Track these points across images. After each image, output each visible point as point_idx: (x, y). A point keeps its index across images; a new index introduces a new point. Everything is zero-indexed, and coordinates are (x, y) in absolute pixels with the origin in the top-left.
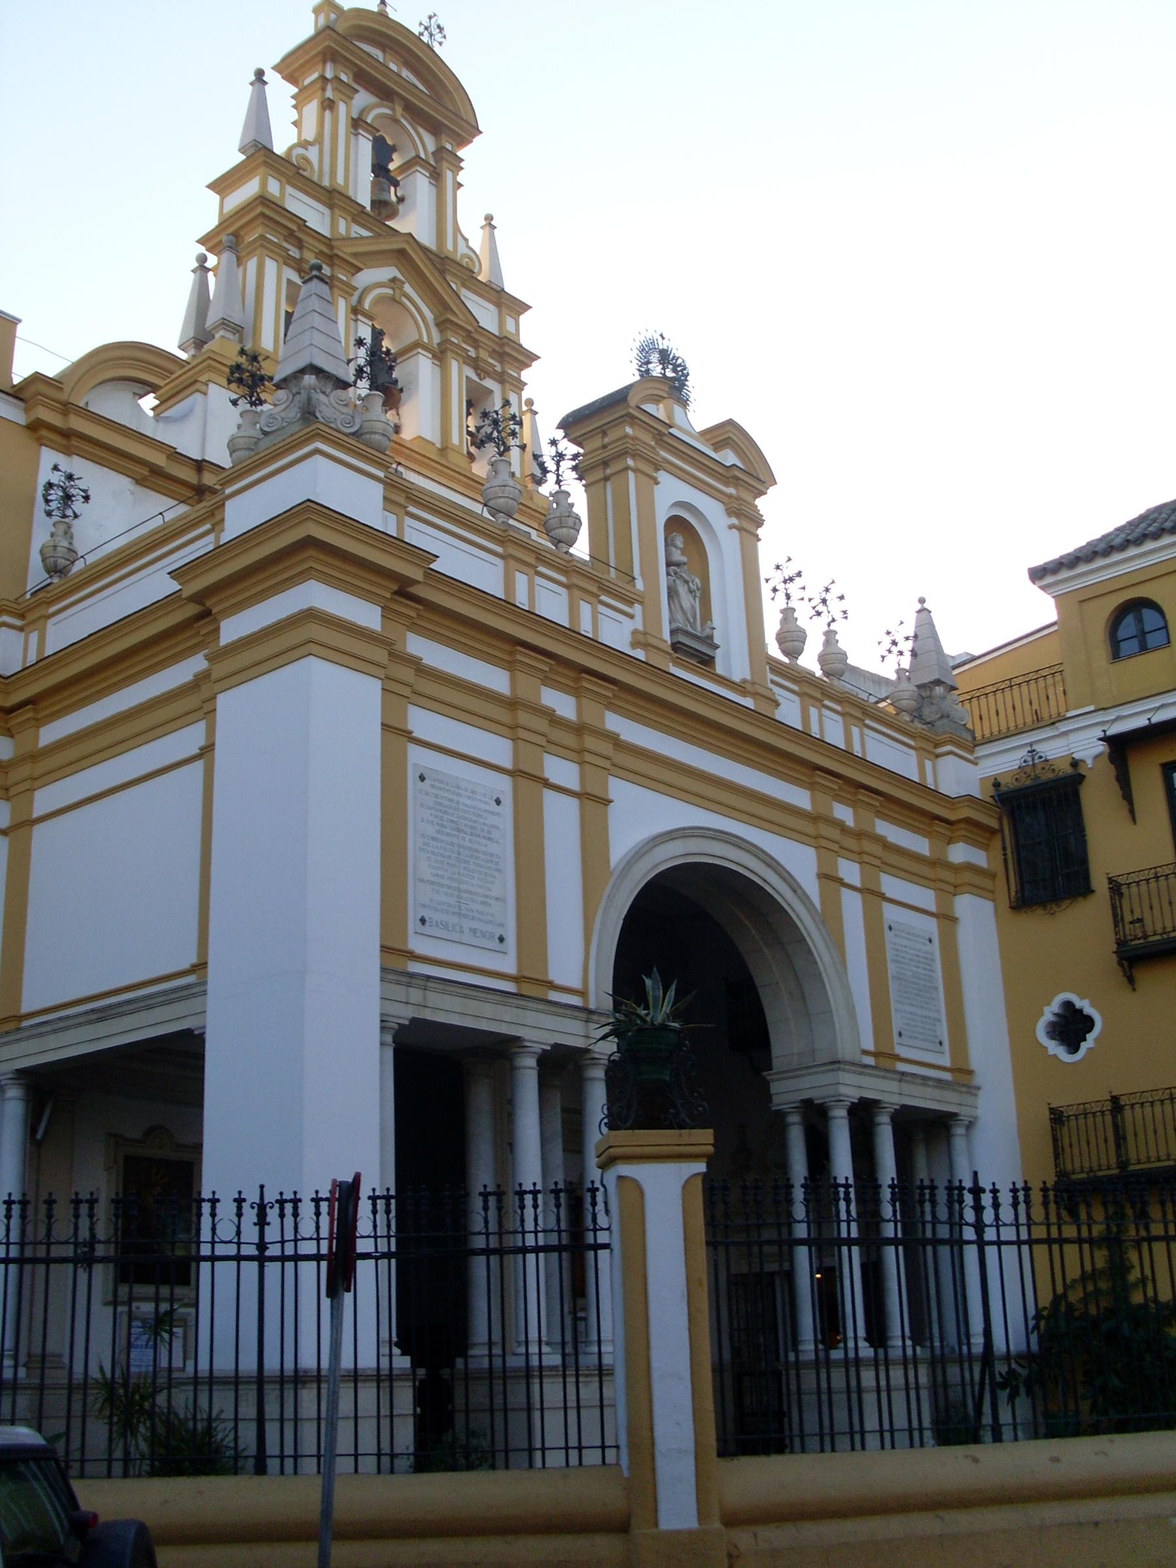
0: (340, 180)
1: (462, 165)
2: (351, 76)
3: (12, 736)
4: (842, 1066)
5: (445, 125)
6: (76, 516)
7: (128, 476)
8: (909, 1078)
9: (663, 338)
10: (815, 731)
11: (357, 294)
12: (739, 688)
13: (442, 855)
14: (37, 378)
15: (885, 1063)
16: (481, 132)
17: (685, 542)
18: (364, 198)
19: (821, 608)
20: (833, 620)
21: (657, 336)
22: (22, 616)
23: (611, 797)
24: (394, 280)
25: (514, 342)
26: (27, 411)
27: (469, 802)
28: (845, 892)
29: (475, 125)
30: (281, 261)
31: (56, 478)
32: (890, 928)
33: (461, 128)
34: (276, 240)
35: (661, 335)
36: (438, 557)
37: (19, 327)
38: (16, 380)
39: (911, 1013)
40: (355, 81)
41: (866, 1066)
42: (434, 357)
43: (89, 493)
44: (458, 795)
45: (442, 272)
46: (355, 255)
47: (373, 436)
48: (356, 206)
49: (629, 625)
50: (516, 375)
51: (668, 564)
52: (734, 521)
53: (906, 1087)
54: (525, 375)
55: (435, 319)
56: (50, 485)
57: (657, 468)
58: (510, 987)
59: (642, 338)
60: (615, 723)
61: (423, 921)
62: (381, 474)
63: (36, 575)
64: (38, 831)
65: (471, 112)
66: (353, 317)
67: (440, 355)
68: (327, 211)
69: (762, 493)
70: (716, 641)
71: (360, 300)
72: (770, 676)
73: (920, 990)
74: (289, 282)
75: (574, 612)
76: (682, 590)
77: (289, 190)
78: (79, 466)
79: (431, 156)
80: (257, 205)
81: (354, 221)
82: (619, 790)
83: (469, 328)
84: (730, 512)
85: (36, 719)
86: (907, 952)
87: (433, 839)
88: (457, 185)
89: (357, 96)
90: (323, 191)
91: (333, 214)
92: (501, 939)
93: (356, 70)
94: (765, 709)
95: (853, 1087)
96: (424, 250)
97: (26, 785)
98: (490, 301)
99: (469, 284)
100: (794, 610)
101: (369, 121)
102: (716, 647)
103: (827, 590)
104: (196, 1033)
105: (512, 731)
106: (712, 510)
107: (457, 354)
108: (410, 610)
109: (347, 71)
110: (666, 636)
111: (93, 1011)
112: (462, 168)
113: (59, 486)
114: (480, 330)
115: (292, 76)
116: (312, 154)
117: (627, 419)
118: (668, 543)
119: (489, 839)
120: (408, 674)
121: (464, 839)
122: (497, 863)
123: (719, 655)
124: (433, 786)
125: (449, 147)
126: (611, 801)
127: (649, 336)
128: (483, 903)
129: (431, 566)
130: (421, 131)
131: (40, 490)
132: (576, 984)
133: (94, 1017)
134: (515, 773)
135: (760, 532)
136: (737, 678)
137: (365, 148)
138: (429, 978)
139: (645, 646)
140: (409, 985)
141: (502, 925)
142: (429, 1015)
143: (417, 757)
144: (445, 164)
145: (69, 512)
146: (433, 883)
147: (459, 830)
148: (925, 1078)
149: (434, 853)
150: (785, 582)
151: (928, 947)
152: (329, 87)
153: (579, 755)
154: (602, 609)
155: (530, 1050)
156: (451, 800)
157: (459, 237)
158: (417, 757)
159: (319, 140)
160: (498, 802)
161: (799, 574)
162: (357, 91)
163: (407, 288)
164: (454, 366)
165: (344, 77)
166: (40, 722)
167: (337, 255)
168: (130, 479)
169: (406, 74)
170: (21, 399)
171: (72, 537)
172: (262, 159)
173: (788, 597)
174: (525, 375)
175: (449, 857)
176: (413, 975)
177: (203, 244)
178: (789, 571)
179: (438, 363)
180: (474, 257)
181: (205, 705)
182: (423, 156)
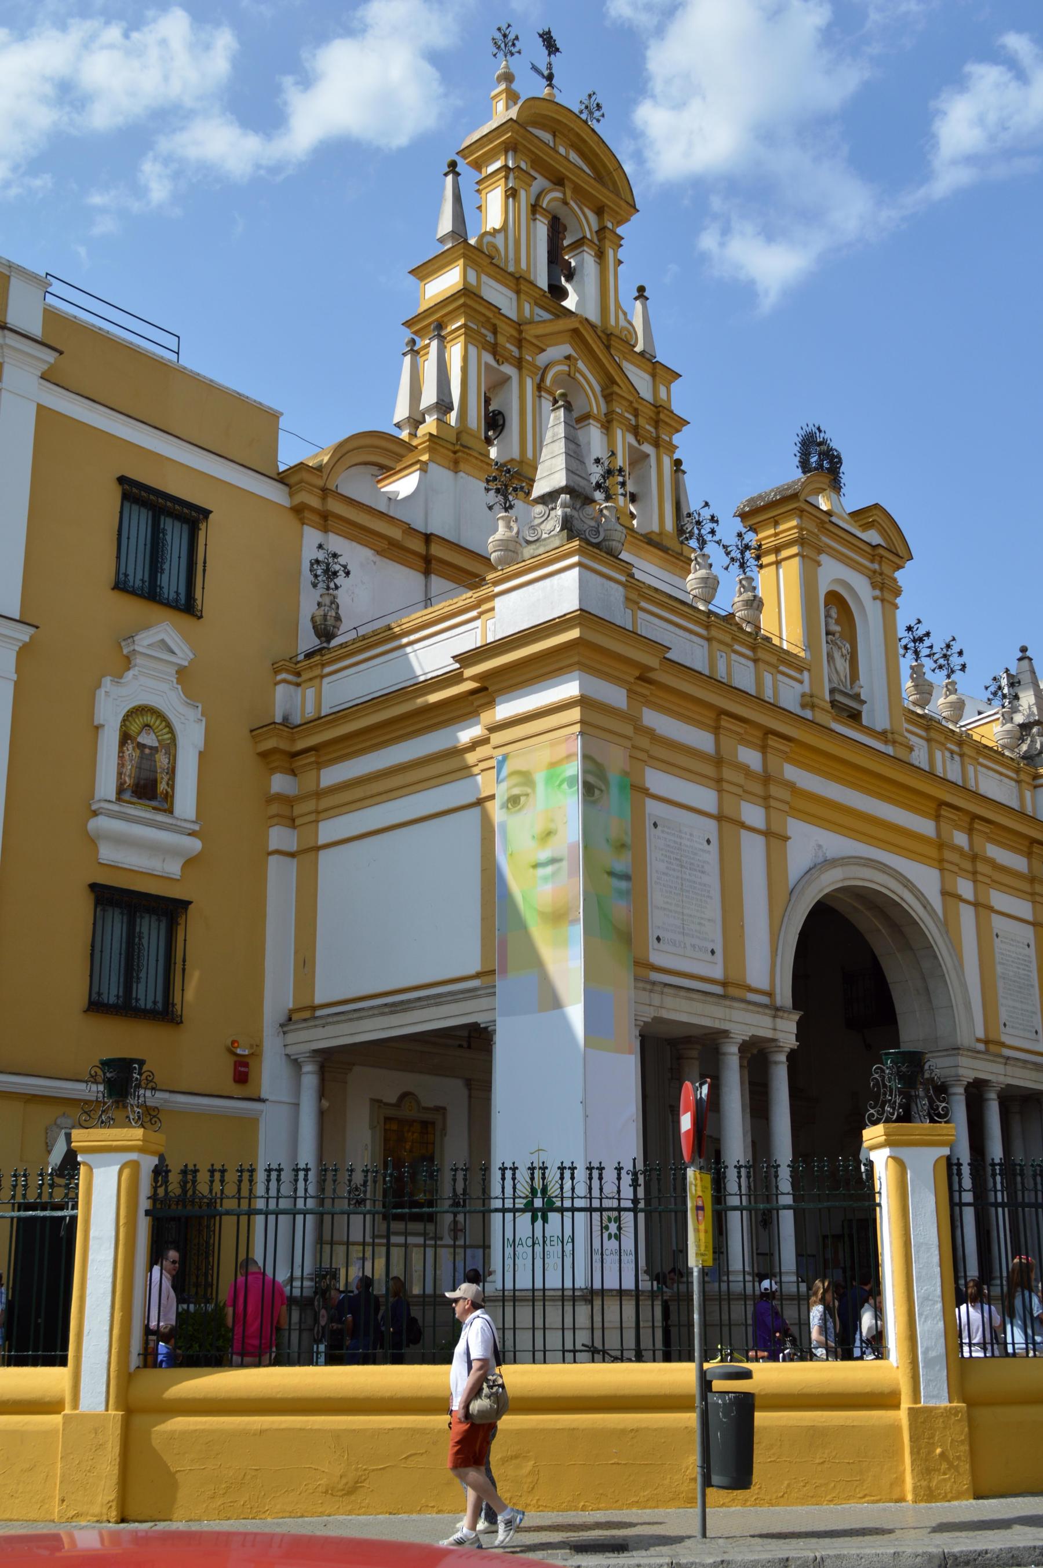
0: (524, 266)
1: (622, 242)
2: (529, 164)
3: (295, 775)
4: (961, 1052)
5: (608, 206)
6: (337, 587)
7: (372, 549)
8: (1012, 1062)
9: (820, 431)
10: (939, 771)
11: (540, 373)
12: (882, 736)
13: (671, 887)
14: (301, 466)
15: (993, 1048)
16: (638, 211)
17: (838, 613)
18: (543, 283)
19: (942, 661)
20: (953, 672)
21: (815, 430)
22: (298, 674)
23: (789, 834)
24: (568, 358)
25: (668, 410)
26: (291, 495)
27: (688, 843)
28: (962, 905)
29: (631, 202)
30: (480, 347)
31: (321, 556)
32: (997, 936)
33: (620, 207)
34: (475, 327)
35: (819, 429)
36: (670, 649)
37: (281, 419)
38: (282, 468)
39: (1014, 1007)
40: (532, 167)
41: (978, 1052)
42: (602, 426)
43: (348, 567)
44: (681, 838)
45: (608, 347)
46: (537, 337)
47: (611, 543)
48: (538, 290)
49: (799, 688)
50: (667, 439)
51: (828, 633)
52: (877, 593)
53: (1010, 1070)
54: (676, 439)
55: (602, 391)
56: (317, 562)
57: (820, 551)
58: (718, 990)
59: (803, 433)
60: (791, 772)
61: (658, 939)
62: (623, 579)
63: (308, 641)
64: (323, 855)
65: (628, 191)
66: (537, 393)
67: (607, 425)
68: (514, 296)
69: (899, 567)
70: (863, 697)
71: (542, 379)
72: (906, 725)
73: (1020, 987)
74: (486, 364)
75: (759, 682)
76: (837, 655)
77: (484, 278)
78: (336, 543)
79: (594, 234)
80: (460, 297)
81: (536, 304)
82: (795, 828)
83: (631, 398)
84: (874, 586)
85: (317, 763)
86: (1010, 956)
87: (666, 874)
88: (617, 262)
89: (535, 183)
90: (510, 278)
91: (519, 299)
92: (713, 952)
93: (533, 157)
94: (901, 754)
95: (970, 1069)
96: (593, 326)
97: (312, 817)
98: (645, 371)
99: (628, 356)
100: (923, 666)
101: (544, 206)
102: (864, 702)
103: (948, 646)
104: (482, 1026)
105: (718, 783)
106: (861, 585)
107: (621, 423)
108: (643, 689)
109: (526, 160)
110: (827, 698)
111: (386, 1005)
112: (621, 245)
113: (324, 562)
114: (640, 400)
115: (477, 163)
116: (499, 241)
117: (798, 512)
118: (828, 616)
119: (703, 872)
120: (644, 742)
121: (685, 873)
122: (709, 891)
123: (865, 709)
124: (663, 832)
125: (610, 225)
126: (789, 838)
127: (809, 430)
128: (700, 924)
129: (668, 655)
130: (586, 210)
131: (306, 566)
132: (765, 985)
133: (387, 1010)
134: (720, 818)
135: (898, 601)
136: (879, 728)
137: (542, 230)
138: (666, 985)
139: (813, 706)
140: (651, 991)
141: (713, 941)
142: (665, 1014)
143: (653, 808)
144: (607, 243)
145: (332, 585)
146: (665, 909)
147: (682, 866)
148: (1025, 1062)
149: (664, 886)
150: (914, 641)
151: (1027, 951)
152: (511, 176)
153: (766, 800)
154: (780, 677)
155: (734, 1040)
156: (675, 842)
157: (620, 312)
158: (653, 808)
160: (708, 842)
161: (928, 634)
162: (536, 179)
163: (580, 364)
164: (619, 433)
165: (523, 165)
166: (320, 765)
167: (525, 339)
168: (373, 552)
169: (573, 156)
170: (286, 485)
171: (338, 607)
172: (462, 251)
173: (916, 653)
174: (676, 439)
175: (676, 888)
176: (654, 983)
177: (408, 327)
178: (920, 632)
179: (605, 431)
180: (632, 330)
181: (480, 764)
182: (589, 236)
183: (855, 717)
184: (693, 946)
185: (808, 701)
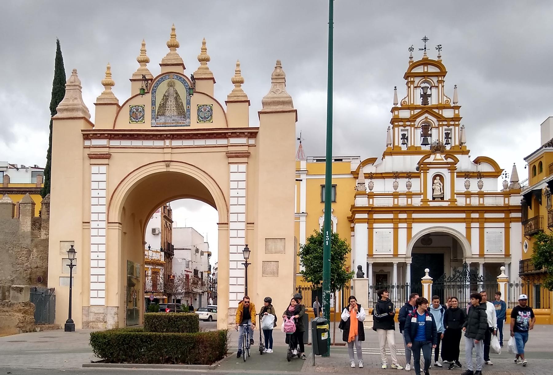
0: (412, 103)
49: (420, 199)
52: (450, 171)
116: (407, 100)
159: (408, 96)
164: (441, 128)
165: (412, 79)
183: (442, 198)
184: (385, 250)
185: (425, 201)
